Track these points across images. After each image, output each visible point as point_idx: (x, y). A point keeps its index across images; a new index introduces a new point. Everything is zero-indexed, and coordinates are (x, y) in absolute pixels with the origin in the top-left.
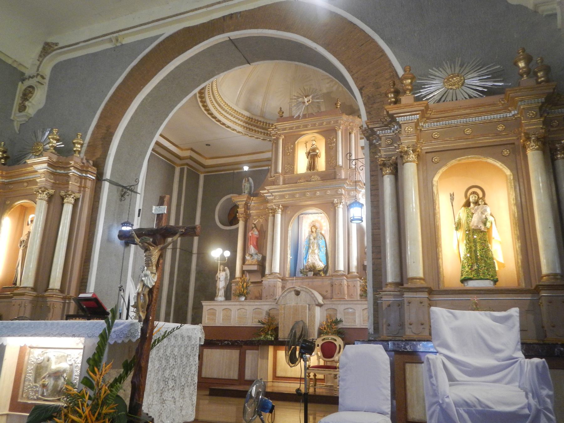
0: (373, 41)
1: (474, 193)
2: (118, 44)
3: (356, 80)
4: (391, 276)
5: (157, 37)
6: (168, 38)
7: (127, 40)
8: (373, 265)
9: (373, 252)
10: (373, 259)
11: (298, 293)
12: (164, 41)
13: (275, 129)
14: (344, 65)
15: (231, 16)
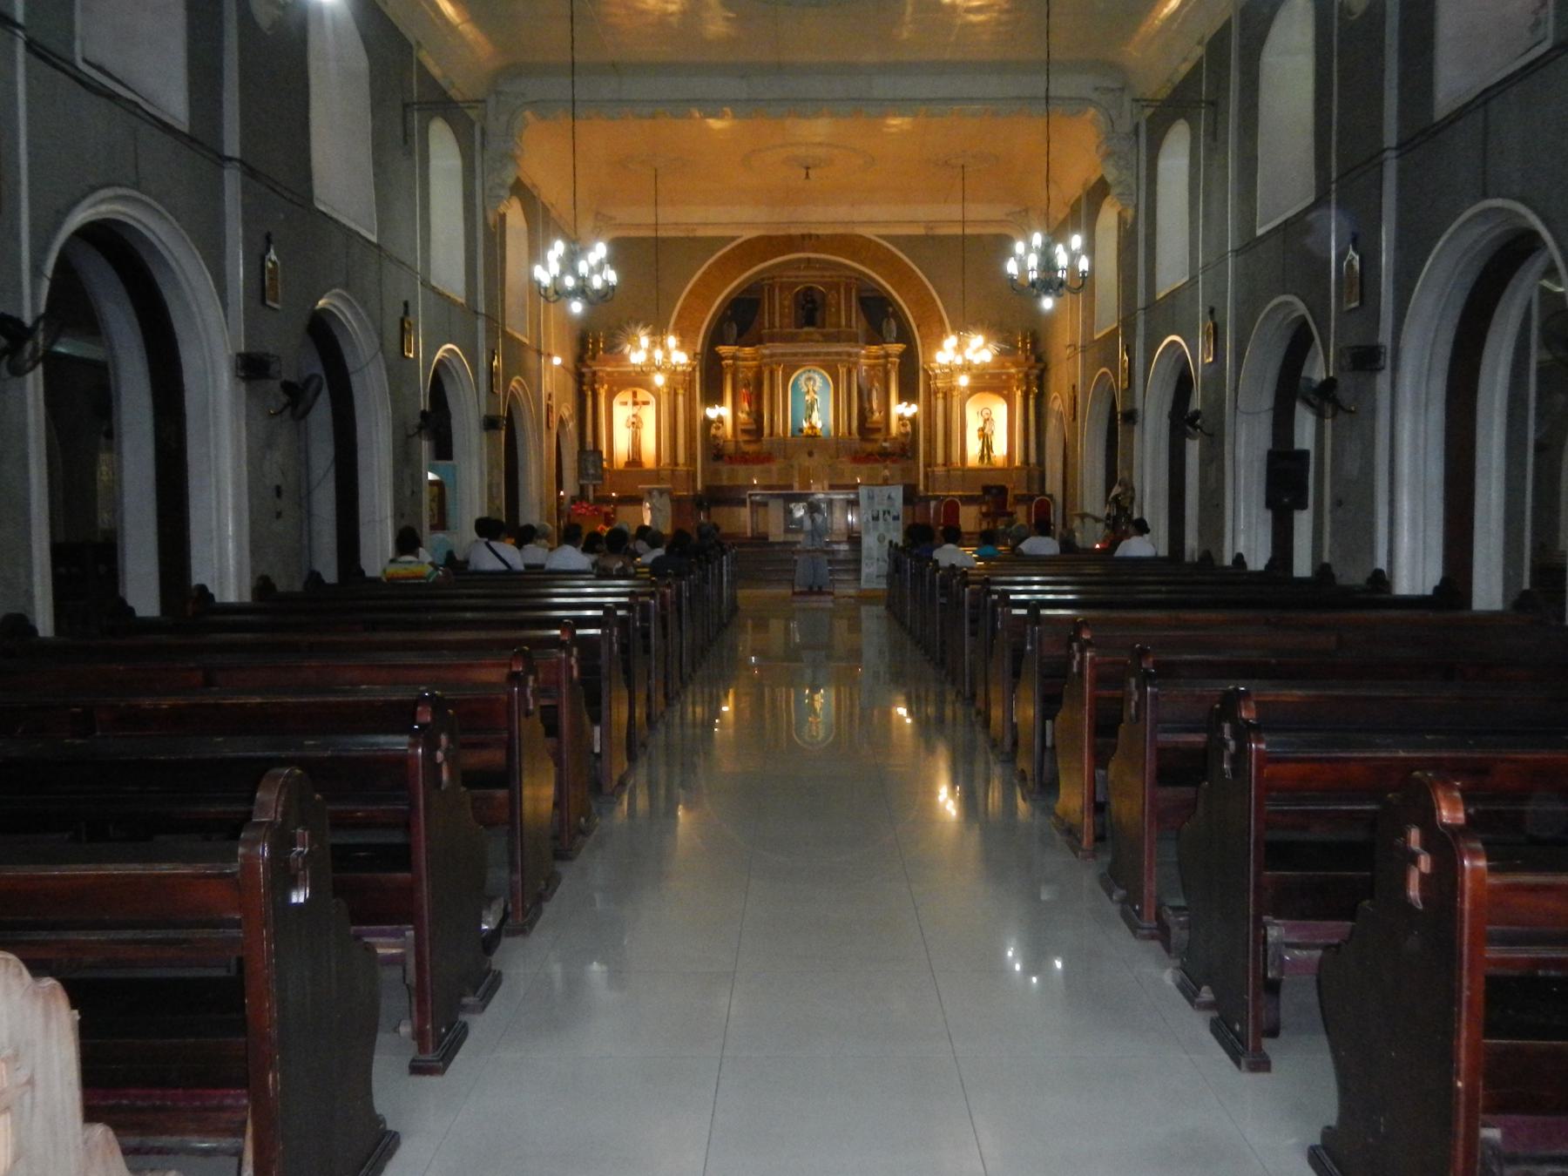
0: (925, 287)
2: (691, 235)
3: (915, 318)
4: (940, 459)
5: (733, 239)
6: (746, 241)
7: (700, 233)
11: (810, 454)
12: (742, 244)
15: (810, 236)
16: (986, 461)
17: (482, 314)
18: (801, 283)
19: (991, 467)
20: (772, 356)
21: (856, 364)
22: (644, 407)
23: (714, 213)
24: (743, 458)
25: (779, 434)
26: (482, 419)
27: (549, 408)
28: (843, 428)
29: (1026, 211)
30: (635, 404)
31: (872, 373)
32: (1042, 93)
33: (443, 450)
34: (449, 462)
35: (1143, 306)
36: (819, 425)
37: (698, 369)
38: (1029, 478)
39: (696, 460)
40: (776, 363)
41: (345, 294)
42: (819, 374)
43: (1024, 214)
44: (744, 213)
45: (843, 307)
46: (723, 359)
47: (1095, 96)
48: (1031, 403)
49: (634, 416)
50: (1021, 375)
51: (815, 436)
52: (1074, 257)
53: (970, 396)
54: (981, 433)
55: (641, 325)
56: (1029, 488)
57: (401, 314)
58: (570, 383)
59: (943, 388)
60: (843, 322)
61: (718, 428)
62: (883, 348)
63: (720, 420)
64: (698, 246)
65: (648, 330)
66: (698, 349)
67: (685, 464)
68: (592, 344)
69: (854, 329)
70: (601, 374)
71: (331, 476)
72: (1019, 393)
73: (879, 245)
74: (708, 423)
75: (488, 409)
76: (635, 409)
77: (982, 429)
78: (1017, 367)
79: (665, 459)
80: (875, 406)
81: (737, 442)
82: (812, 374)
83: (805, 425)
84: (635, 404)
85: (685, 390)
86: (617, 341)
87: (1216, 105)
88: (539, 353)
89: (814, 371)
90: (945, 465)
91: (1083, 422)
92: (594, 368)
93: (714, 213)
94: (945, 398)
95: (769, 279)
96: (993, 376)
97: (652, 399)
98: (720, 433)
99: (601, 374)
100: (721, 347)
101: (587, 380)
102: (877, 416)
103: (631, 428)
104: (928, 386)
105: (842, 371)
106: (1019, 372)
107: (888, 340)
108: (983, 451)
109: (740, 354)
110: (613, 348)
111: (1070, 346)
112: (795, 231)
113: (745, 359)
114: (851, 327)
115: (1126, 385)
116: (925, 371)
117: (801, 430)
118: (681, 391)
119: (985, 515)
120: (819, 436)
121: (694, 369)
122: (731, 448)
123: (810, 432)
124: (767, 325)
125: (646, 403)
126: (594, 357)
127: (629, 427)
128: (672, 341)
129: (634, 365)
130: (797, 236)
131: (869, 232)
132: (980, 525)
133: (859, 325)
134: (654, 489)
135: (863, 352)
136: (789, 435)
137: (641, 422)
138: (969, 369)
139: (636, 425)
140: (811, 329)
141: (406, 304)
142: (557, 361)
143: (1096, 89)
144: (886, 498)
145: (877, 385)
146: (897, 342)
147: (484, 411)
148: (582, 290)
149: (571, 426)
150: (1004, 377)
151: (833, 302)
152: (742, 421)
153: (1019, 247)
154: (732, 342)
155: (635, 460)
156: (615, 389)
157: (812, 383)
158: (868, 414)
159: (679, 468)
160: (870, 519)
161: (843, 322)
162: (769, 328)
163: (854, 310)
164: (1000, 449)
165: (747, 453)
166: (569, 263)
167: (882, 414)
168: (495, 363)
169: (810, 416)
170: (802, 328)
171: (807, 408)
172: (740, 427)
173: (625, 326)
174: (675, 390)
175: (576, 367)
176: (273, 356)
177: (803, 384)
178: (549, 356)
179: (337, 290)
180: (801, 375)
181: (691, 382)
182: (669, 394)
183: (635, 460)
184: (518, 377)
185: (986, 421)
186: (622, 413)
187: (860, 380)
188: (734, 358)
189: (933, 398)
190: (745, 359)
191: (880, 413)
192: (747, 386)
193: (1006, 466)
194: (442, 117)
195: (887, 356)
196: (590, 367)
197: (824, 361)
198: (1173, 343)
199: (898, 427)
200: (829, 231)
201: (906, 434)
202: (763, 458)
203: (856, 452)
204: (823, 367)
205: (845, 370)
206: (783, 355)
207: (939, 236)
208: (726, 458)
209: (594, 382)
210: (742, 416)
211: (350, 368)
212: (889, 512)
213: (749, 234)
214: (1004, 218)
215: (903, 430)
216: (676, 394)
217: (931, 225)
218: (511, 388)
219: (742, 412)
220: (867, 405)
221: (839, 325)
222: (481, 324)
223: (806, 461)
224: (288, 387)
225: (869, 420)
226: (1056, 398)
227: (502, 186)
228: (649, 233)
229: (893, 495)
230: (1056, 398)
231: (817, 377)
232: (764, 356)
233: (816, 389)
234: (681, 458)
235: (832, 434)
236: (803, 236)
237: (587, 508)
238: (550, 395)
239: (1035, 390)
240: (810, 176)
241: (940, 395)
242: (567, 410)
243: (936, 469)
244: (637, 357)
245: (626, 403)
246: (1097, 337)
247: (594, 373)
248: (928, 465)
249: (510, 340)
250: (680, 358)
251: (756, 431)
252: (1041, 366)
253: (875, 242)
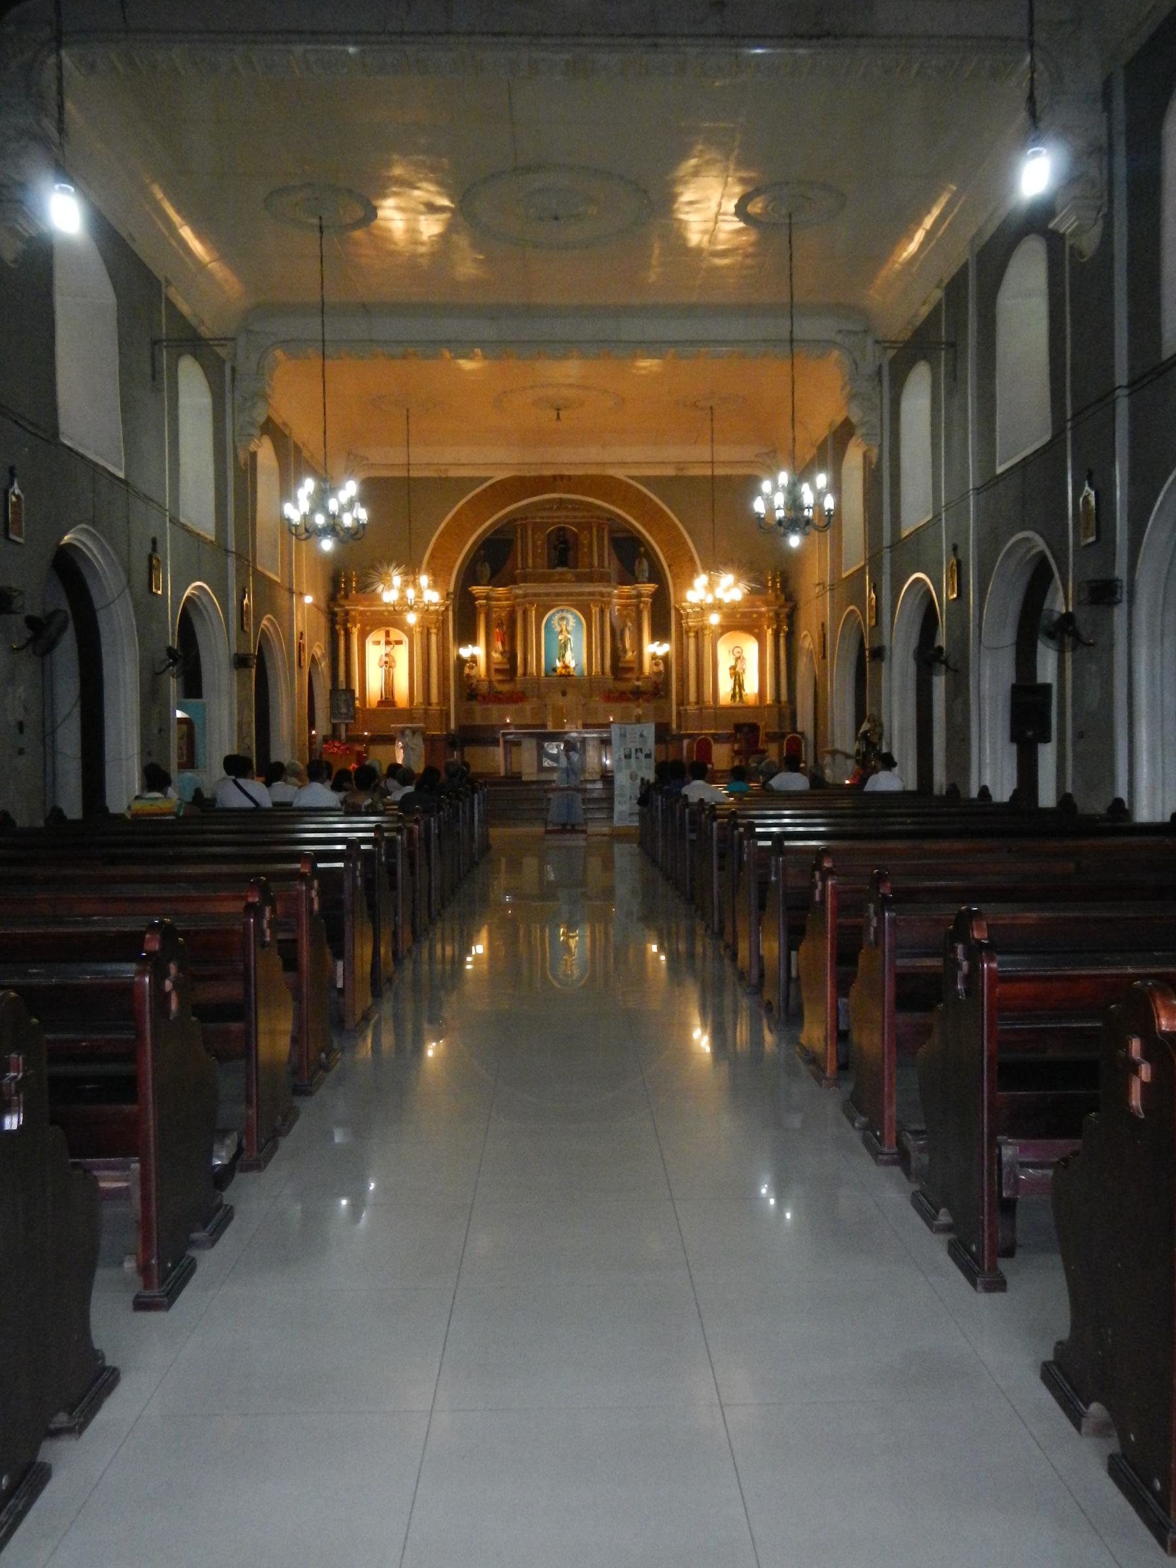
1: (739, 652)
2: (444, 476)
3: (666, 558)
4: (692, 697)
6: (498, 482)
7: (454, 473)
11: (564, 694)
14: (658, 545)
15: (562, 477)
16: (738, 699)
17: (232, 552)
18: (554, 524)
19: (744, 705)
20: (525, 596)
21: (609, 603)
22: (396, 646)
23: (466, 453)
24: (496, 697)
25: (532, 673)
26: (232, 656)
27: (301, 648)
28: (596, 668)
29: (774, 451)
30: (388, 643)
31: (625, 612)
32: (787, 336)
33: (193, 688)
34: (200, 700)
35: (888, 545)
36: (572, 664)
37: (451, 608)
38: (781, 715)
39: (449, 700)
40: (529, 603)
41: (91, 529)
42: (572, 613)
43: (772, 455)
44: (500, 454)
45: (595, 548)
46: (477, 599)
47: (839, 338)
48: (782, 641)
49: (387, 655)
50: (771, 614)
51: (569, 675)
52: (819, 495)
53: (722, 634)
54: (732, 671)
55: (394, 564)
56: (780, 727)
57: (150, 551)
58: (323, 621)
59: (695, 627)
60: (596, 563)
61: (471, 668)
62: (636, 588)
63: (474, 659)
64: (454, 486)
65: (401, 570)
66: (451, 589)
67: (438, 704)
68: (345, 583)
69: (607, 570)
70: (353, 613)
71: (77, 711)
72: (770, 631)
73: (631, 486)
74: (461, 662)
75: (238, 647)
76: (389, 648)
77: (733, 668)
78: (767, 606)
79: (418, 698)
80: (628, 645)
81: (490, 682)
82: (564, 614)
83: (558, 664)
84: (388, 643)
85: (438, 630)
86: (370, 581)
87: (955, 347)
88: (291, 591)
89: (568, 611)
90: (697, 703)
91: (832, 659)
92: (347, 607)
93: (466, 453)
94: (696, 636)
95: (522, 519)
96: (744, 615)
97: (405, 639)
98: (473, 672)
99: (353, 613)
100: (474, 587)
101: (339, 619)
102: (630, 655)
103: (384, 667)
104: (679, 625)
105: (595, 610)
106: (769, 611)
107: (640, 580)
108: (734, 689)
109: (493, 594)
110: (365, 587)
111: (819, 584)
112: (548, 472)
113: (498, 600)
114: (603, 567)
115: (873, 623)
116: (677, 610)
117: (554, 670)
118: (434, 631)
119: (737, 753)
120: (572, 676)
121: (447, 609)
122: (484, 687)
123: (563, 671)
124: (520, 566)
125: (399, 642)
126: (346, 597)
127: (381, 667)
128: (424, 580)
129: (386, 604)
130: (549, 477)
131: (619, 473)
132: (733, 762)
133: (611, 566)
134: (408, 728)
135: (616, 591)
136: (543, 674)
137: (394, 662)
138: (720, 608)
139: (388, 664)
140: (565, 569)
141: (154, 541)
142: (308, 599)
143: (840, 331)
144: (638, 736)
145: (629, 624)
146: (650, 581)
147: (234, 650)
148: (333, 528)
149: (324, 665)
150: (755, 616)
151: (585, 542)
152: (495, 661)
153: (766, 486)
154: (485, 580)
155: (388, 700)
156: (368, 628)
157: (565, 622)
158: (621, 654)
159: (432, 708)
160: (623, 757)
161: (596, 563)
162: (522, 568)
163: (606, 549)
164: (751, 687)
165: (501, 693)
166: (319, 500)
167: (635, 653)
168: (246, 601)
169: (563, 656)
170: (554, 568)
171: (561, 647)
172: (494, 667)
173: (378, 565)
174: (428, 630)
175: (328, 606)
176: (15, 591)
177: (557, 624)
178: (301, 594)
179: (84, 526)
180: (553, 615)
181: (444, 622)
182: (422, 633)
183: (388, 700)
184: (269, 616)
185: (737, 659)
186: (374, 652)
187: (613, 620)
188: (487, 598)
189: (685, 636)
190: (498, 600)
191: (633, 652)
192: (500, 625)
193: (758, 704)
194: (191, 354)
195: (639, 595)
196: (342, 606)
197: (573, 600)
198: (918, 580)
199: (651, 667)
200: (580, 472)
201: (658, 674)
202: (516, 698)
203: (610, 691)
204: (572, 606)
205: (598, 609)
206: (535, 595)
207: (686, 477)
208: (480, 698)
209: (346, 621)
210: (496, 656)
211: (97, 606)
212: (641, 750)
213: (500, 475)
214: (753, 459)
215: (655, 669)
216: (429, 633)
217: (682, 466)
218: (262, 626)
219: (496, 652)
220: (620, 645)
221: (591, 565)
222: (232, 562)
223: (560, 701)
224: (31, 622)
225: (621, 659)
226: (806, 636)
227: (252, 424)
228: (402, 473)
229: (645, 733)
230: (806, 636)
231: (570, 616)
232: (517, 597)
233: (569, 628)
234: (434, 697)
235: (586, 674)
236: (555, 478)
237: (339, 747)
238: (302, 634)
239: (785, 628)
240: (561, 416)
241: (692, 634)
242: (319, 649)
243: (688, 707)
244: (389, 596)
245: (378, 643)
246: (844, 575)
247: (347, 613)
248: (682, 702)
249: (260, 578)
250: (433, 597)
251: (509, 671)
252: (791, 604)
253: (626, 483)
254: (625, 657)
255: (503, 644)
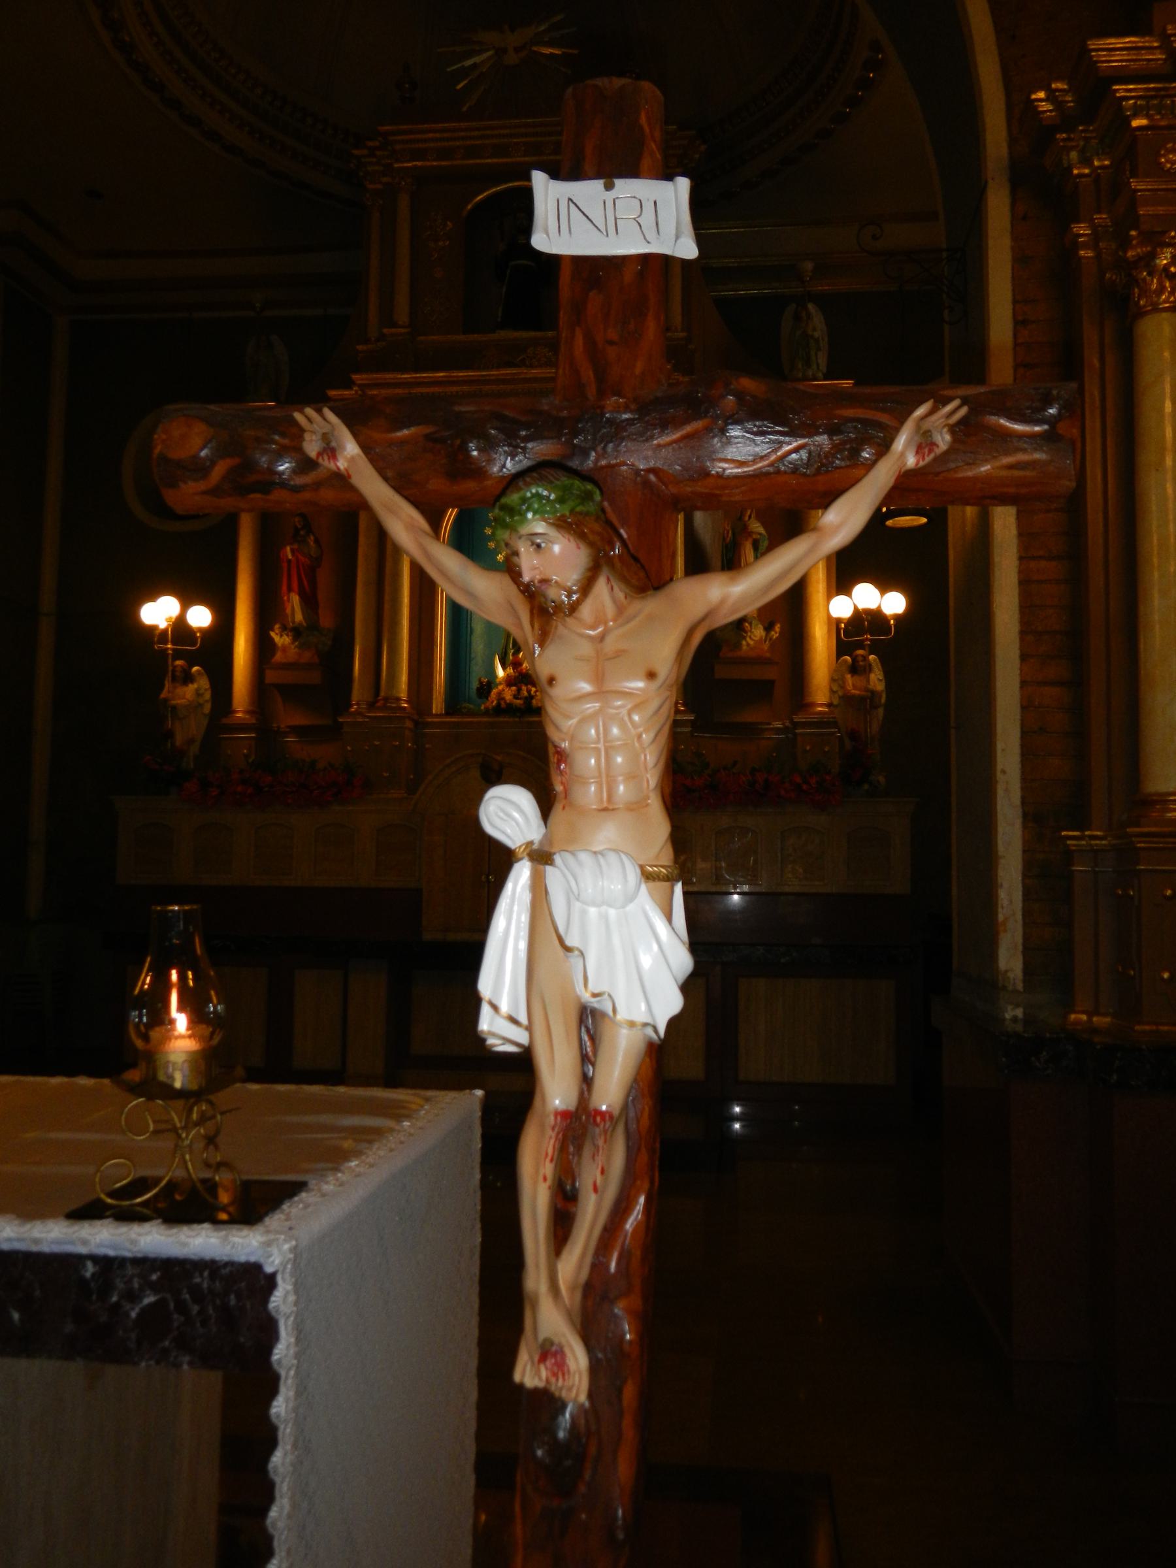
8: (1024, 708)
9: (1024, 657)
10: (1024, 684)
13: (378, 153)
117: (485, 689)
167: (775, 634)
191: (769, 628)
199: (836, 679)
201: (866, 701)
219: (284, 628)
254: (738, 645)
255: (310, 602)
